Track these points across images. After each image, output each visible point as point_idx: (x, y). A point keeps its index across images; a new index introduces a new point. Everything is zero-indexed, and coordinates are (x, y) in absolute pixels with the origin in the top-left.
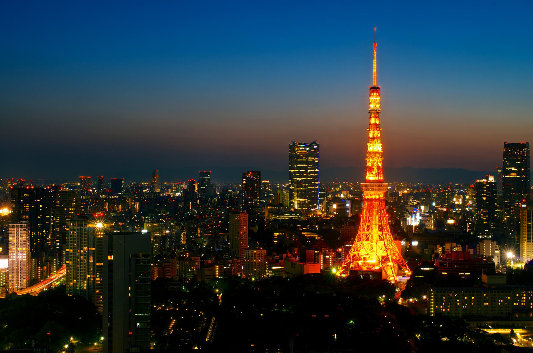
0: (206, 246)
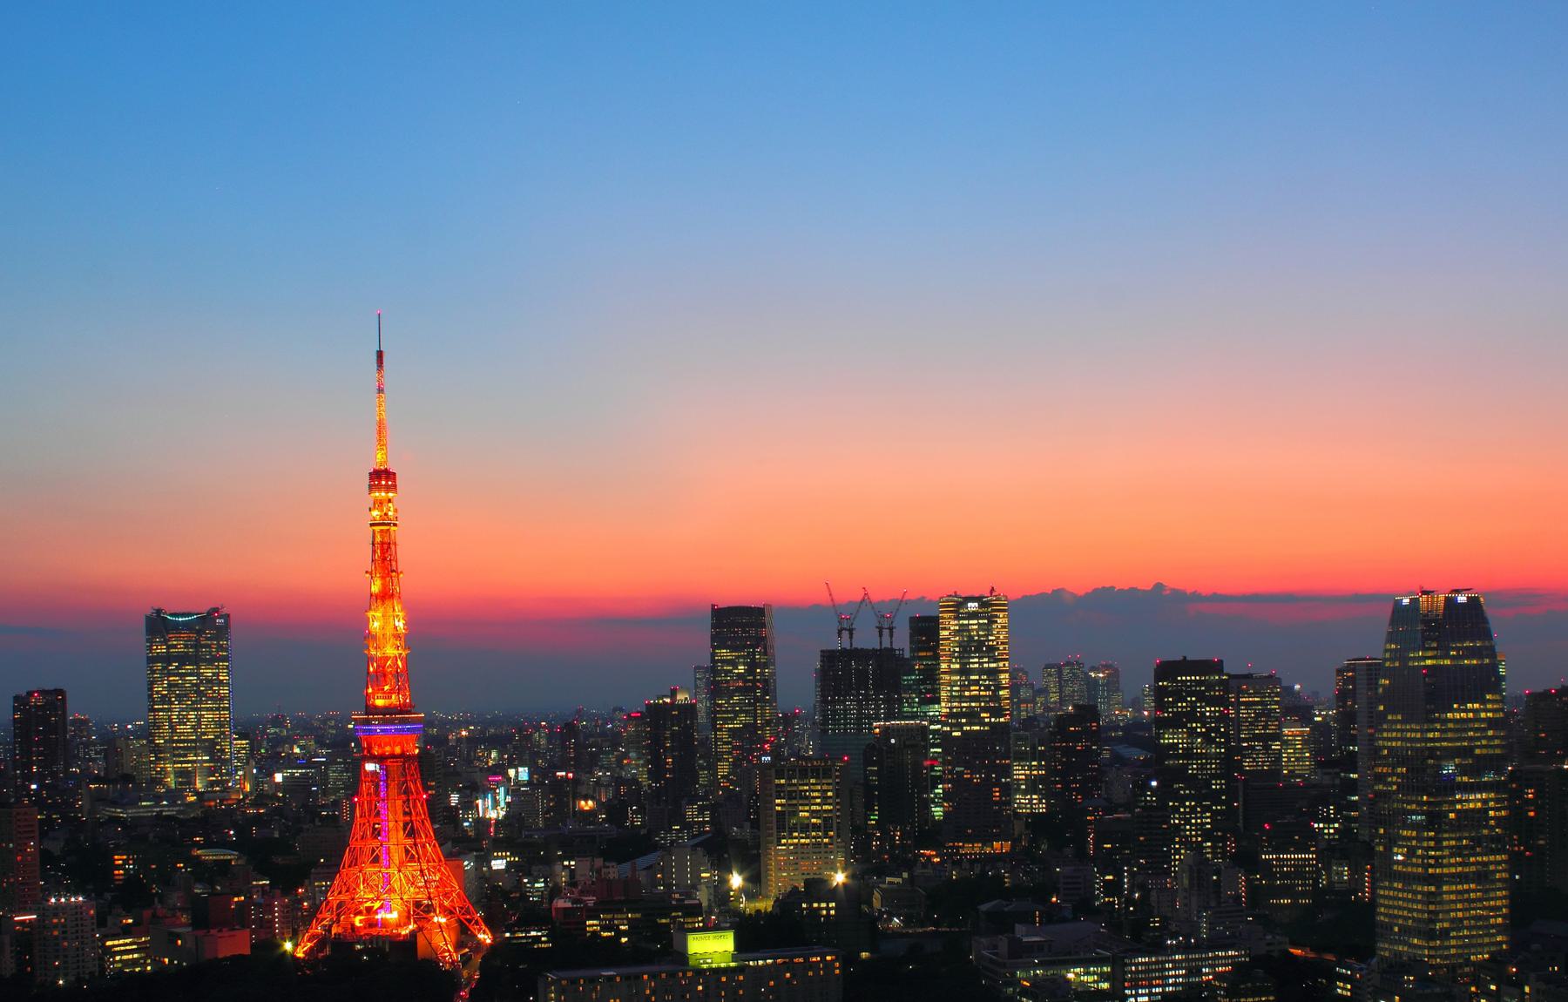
0: (76, 894)
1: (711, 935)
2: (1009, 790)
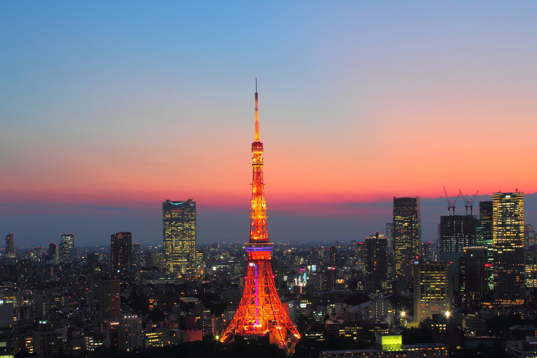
1: (392, 337)
2: (524, 277)
